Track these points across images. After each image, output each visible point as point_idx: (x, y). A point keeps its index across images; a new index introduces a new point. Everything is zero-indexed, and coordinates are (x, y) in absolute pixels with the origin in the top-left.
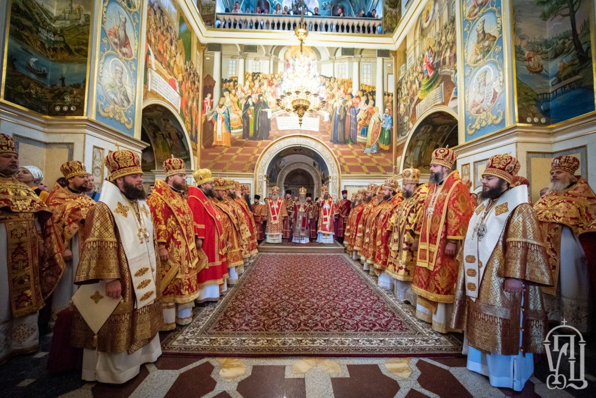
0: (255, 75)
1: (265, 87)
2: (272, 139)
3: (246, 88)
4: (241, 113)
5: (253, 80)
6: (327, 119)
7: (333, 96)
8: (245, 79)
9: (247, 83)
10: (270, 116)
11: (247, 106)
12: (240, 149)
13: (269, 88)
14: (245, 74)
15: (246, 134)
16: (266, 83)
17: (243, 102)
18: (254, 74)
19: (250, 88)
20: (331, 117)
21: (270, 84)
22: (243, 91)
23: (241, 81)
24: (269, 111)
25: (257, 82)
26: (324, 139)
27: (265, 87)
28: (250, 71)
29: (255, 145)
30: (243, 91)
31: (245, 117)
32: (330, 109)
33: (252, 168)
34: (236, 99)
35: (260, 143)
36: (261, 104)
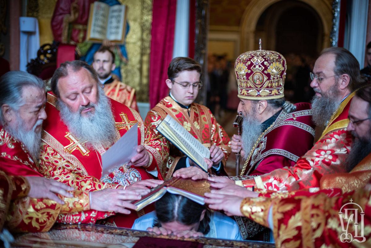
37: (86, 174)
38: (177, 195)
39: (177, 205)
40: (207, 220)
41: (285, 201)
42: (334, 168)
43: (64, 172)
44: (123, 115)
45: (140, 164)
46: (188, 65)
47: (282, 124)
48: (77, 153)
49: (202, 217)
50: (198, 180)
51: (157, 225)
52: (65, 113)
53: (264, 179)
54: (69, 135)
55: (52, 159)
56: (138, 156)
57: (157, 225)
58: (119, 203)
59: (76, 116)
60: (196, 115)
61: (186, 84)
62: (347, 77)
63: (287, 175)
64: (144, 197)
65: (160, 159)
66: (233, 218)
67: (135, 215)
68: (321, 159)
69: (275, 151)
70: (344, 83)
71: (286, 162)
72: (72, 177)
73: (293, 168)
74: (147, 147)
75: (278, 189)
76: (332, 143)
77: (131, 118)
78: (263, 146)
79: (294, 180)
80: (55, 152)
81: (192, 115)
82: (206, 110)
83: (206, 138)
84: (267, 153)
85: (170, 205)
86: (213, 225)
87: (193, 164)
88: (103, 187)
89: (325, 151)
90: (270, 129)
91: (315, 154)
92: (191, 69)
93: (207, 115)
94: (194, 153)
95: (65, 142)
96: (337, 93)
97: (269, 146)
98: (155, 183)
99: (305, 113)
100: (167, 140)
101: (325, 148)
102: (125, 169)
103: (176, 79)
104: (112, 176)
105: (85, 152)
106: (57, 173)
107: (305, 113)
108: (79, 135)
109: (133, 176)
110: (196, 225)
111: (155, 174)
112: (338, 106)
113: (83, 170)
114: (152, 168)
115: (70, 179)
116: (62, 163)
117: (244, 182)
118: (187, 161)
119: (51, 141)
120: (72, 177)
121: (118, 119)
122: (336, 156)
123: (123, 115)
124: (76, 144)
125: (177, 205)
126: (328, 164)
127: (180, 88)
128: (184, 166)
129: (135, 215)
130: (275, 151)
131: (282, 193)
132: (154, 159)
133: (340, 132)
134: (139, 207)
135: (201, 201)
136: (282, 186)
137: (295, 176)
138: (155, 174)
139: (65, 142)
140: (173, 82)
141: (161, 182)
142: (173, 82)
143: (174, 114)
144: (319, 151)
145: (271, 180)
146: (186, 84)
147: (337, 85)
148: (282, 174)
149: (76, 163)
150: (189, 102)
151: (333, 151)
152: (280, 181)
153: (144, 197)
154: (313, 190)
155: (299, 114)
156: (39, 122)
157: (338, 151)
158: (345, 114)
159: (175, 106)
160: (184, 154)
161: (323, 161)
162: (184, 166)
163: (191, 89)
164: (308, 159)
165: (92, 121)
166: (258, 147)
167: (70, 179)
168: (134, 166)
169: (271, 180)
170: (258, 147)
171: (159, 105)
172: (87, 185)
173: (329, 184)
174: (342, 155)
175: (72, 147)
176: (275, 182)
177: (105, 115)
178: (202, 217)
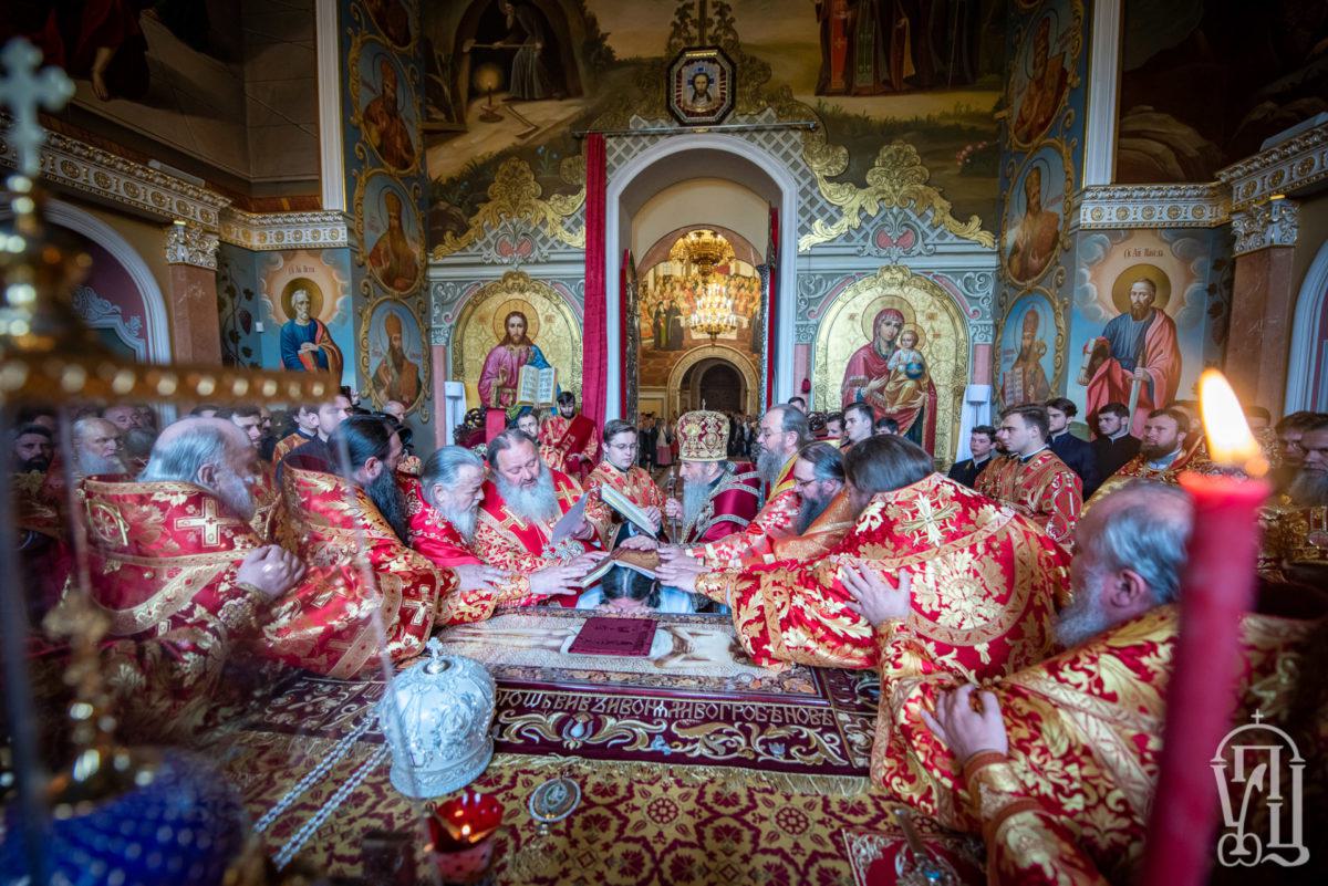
0: (667, 278)
1: (678, 292)
2: (685, 349)
3: (657, 293)
4: (652, 321)
5: (664, 284)
6: (745, 326)
7: (753, 299)
8: (656, 283)
9: (658, 288)
10: (683, 324)
11: (658, 313)
12: (652, 362)
13: (682, 293)
14: (656, 277)
15: (657, 344)
16: (678, 286)
17: (654, 309)
18: (665, 277)
19: (662, 293)
20: (750, 323)
21: (683, 288)
22: (653, 297)
23: (651, 286)
24: (682, 319)
25: (668, 287)
26: (742, 349)
27: (678, 292)
28: (661, 274)
29: (668, 356)
30: (653, 297)
31: (656, 326)
32: (749, 313)
33: (665, 382)
34: (646, 307)
35: (672, 354)
36: (673, 311)
37: (525, 550)
38: (626, 569)
39: (625, 579)
40: (657, 592)
41: (744, 577)
42: (785, 530)
43: (500, 551)
44: (561, 484)
45: (584, 536)
46: (623, 427)
47: (729, 487)
48: (515, 529)
49: (652, 590)
50: (646, 551)
51: (603, 602)
52: (503, 489)
53: (715, 547)
54: (505, 509)
55: (486, 537)
56: (583, 526)
57: (603, 602)
58: (563, 583)
59: (515, 490)
60: (635, 479)
61: (623, 447)
62: (795, 435)
63: (738, 541)
64: (589, 572)
65: (601, 529)
66: (690, 595)
67: (580, 591)
68: (772, 522)
69: (726, 517)
70: (791, 440)
71: (735, 527)
72: (510, 555)
73: (744, 533)
74: (590, 518)
75: (730, 556)
76: (782, 505)
77: (570, 486)
78: (710, 511)
79: (746, 546)
80: (490, 529)
81: (631, 478)
82: (644, 472)
83: (647, 502)
84: (718, 519)
85: (618, 579)
86: (663, 597)
87: (637, 528)
88: (545, 564)
89: (776, 513)
90: (715, 491)
91: (766, 517)
92: (626, 430)
93: (646, 478)
94: (636, 517)
95: (501, 517)
96: (784, 450)
97: (718, 511)
98: (602, 555)
99: (751, 475)
100: (610, 507)
101: (776, 510)
102: (567, 540)
103: (612, 442)
104: (553, 550)
105: (523, 527)
106: (492, 552)
107: (751, 475)
108: (518, 507)
109: (576, 548)
110: (646, 599)
111: (598, 544)
112: (785, 467)
113: (522, 547)
114: (594, 539)
115: (508, 558)
116: (497, 541)
117: (694, 551)
118: (630, 526)
119: (488, 518)
120: (510, 555)
121: (558, 488)
122: (787, 518)
123: (561, 484)
124: (514, 518)
125: (625, 579)
126: (780, 527)
127: (616, 450)
128: (628, 536)
129: (580, 591)
130: (726, 517)
131: (737, 565)
132: (596, 532)
133: (791, 493)
134: (585, 583)
135: (651, 575)
136: (734, 553)
137: (748, 542)
138: (598, 544)
139: (501, 517)
140: (609, 445)
141: (608, 554)
142: (609, 445)
143: (613, 478)
144: (769, 514)
145: (723, 547)
146: (623, 447)
147: (783, 442)
148: (733, 540)
149: (514, 539)
150: (626, 465)
151: (784, 513)
152: (732, 548)
153: (589, 572)
154: (769, 559)
155: (745, 476)
156: (476, 503)
157: (790, 513)
158: (791, 475)
159: (614, 471)
160: (626, 519)
161: (775, 525)
162: (628, 536)
163: (627, 450)
164: (759, 523)
165: (533, 495)
166: (704, 511)
167: (508, 558)
168: (575, 537)
169: (723, 547)
170: (704, 511)
171: (596, 470)
172: (526, 564)
173: (783, 550)
174: (794, 517)
175: (508, 522)
176: (727, 549)
177: (547, 487)
178: (652, 590)
